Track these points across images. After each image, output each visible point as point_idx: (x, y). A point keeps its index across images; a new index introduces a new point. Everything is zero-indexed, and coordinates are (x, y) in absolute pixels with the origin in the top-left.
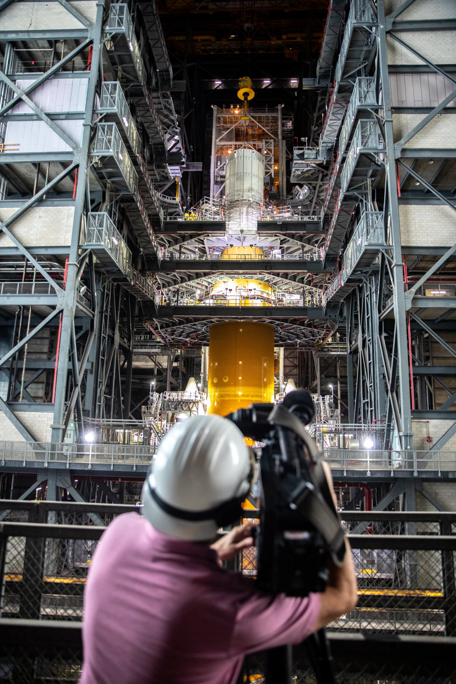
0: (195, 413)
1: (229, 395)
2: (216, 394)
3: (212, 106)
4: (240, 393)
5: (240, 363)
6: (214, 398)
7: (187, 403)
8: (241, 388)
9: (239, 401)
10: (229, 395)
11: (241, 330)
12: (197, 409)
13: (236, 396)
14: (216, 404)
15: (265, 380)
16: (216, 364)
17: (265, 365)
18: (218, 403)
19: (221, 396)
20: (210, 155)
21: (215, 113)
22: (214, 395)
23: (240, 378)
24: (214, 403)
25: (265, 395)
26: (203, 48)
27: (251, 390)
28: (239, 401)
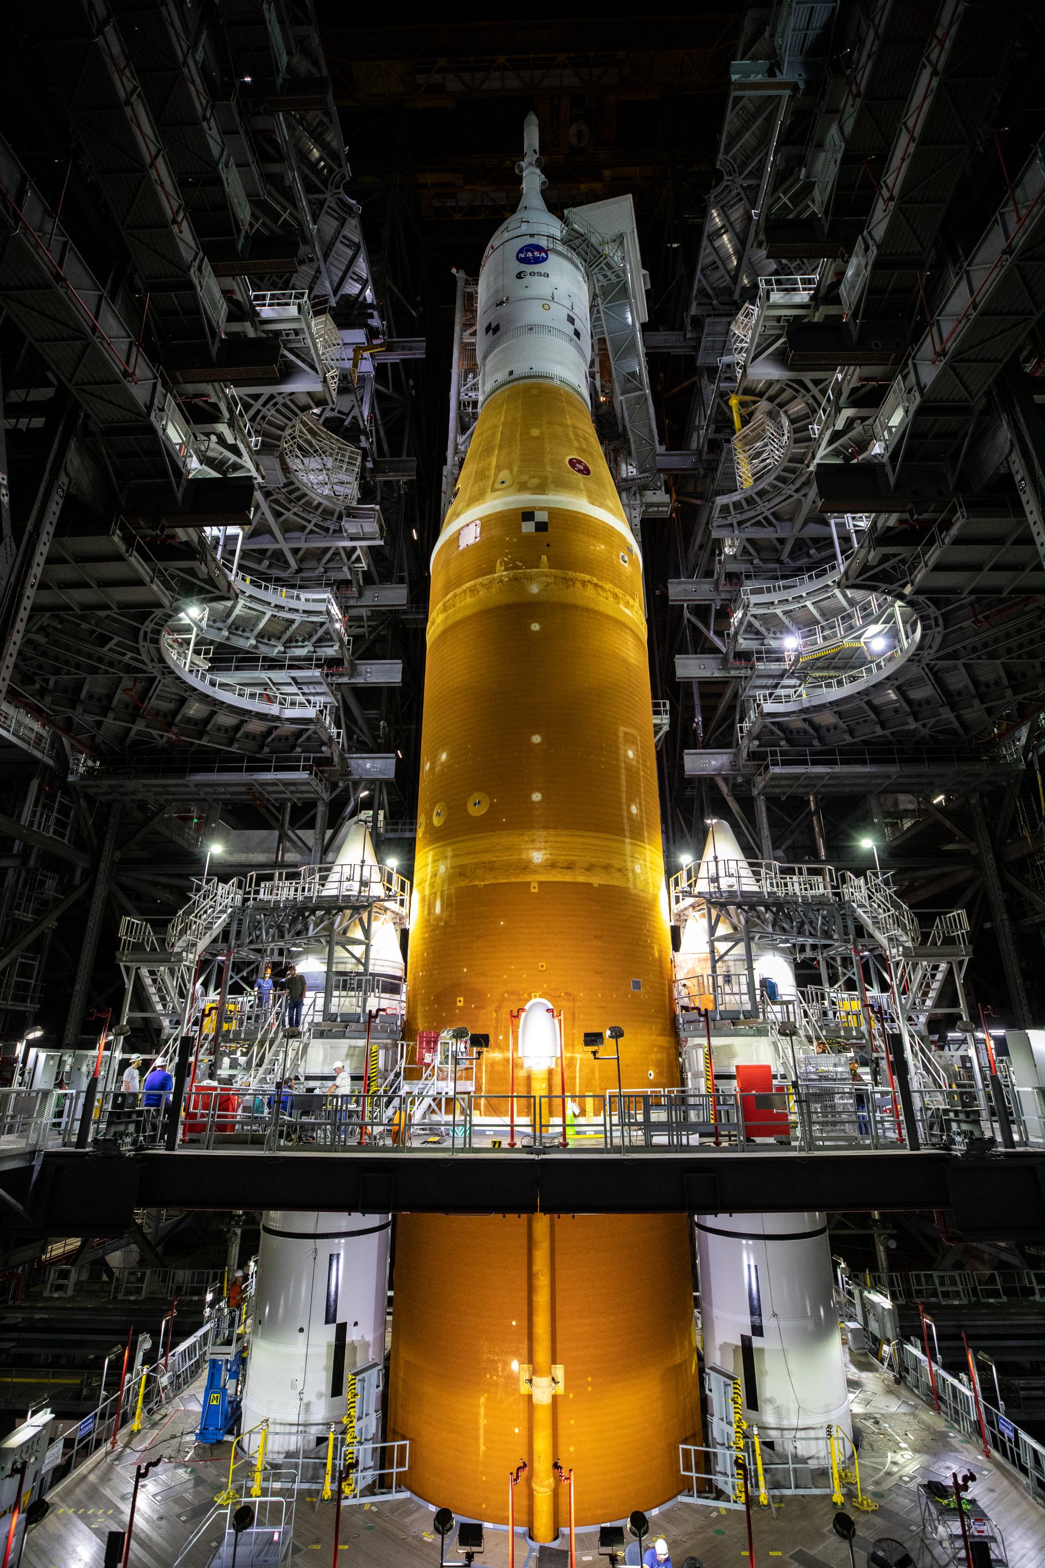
0: (358, 950)
1: (490, 867)
2: (442, 869)
3: (454, 271)
4: (538, 857)
5: (536, 739)
6: (432, 885)
7: (328, 911)
8: (541, 834)
9: (534, 890)
10: (490, 867)
11: (535, 627)
12: (367, 932)
13: (526, 867)
14: (438, 910)
15: (634, 809)
16: (444, 757)
17: (631, 754)
18: (447, 905)
19: (459, 873)
20: (450, 366)
21: (460, 284)
22: (435, 875)
23: (537, 797)
24: (431, 907)
25: (638, 869)
26: (436, 204)
27: (580, 845)
28: (534, 890)
